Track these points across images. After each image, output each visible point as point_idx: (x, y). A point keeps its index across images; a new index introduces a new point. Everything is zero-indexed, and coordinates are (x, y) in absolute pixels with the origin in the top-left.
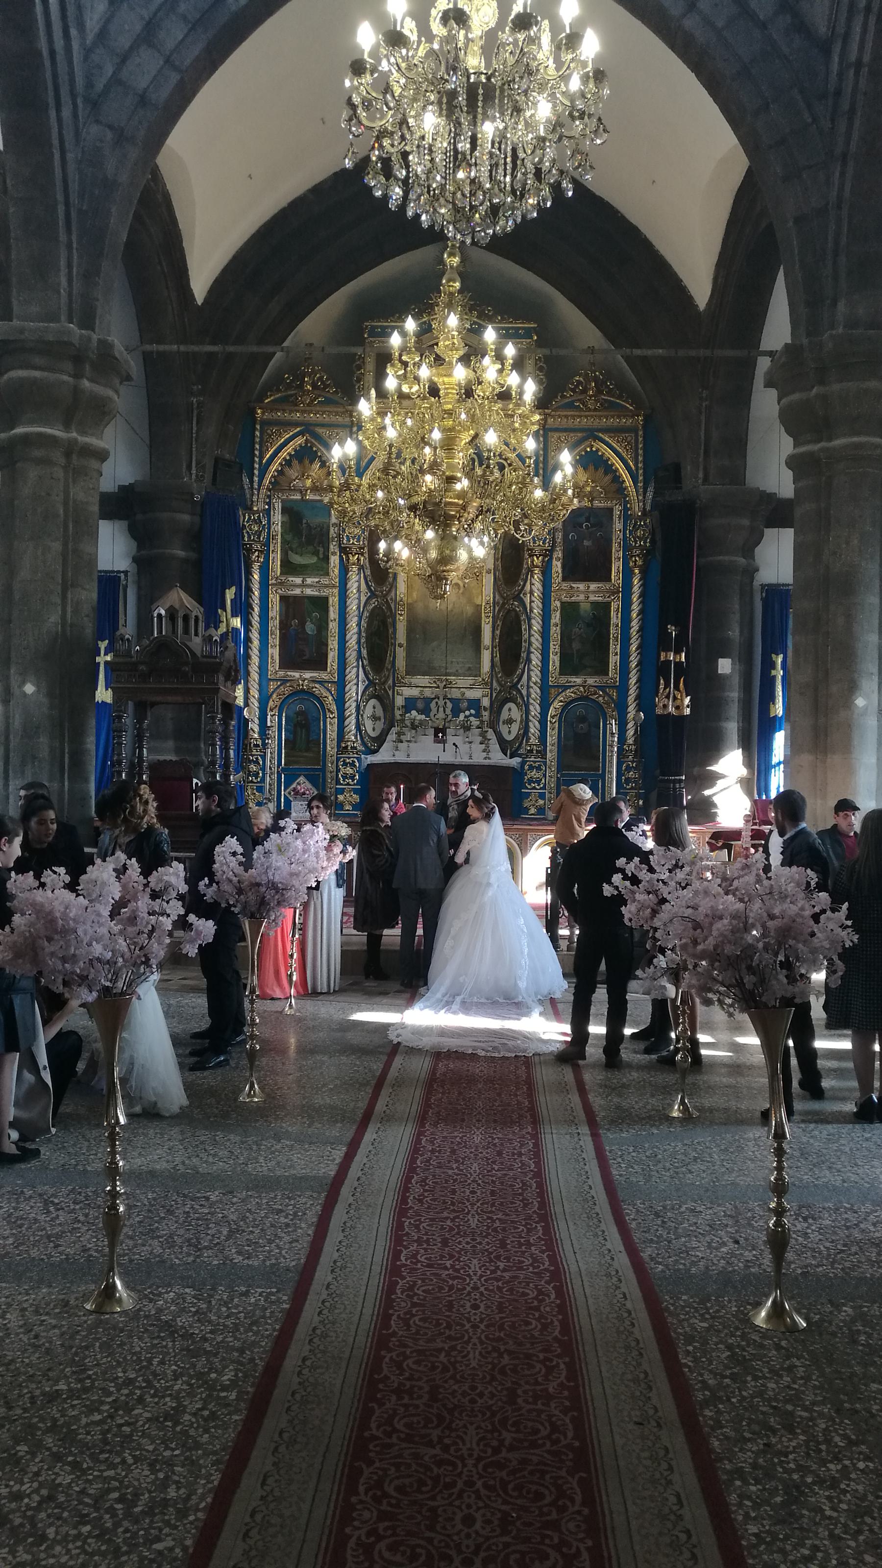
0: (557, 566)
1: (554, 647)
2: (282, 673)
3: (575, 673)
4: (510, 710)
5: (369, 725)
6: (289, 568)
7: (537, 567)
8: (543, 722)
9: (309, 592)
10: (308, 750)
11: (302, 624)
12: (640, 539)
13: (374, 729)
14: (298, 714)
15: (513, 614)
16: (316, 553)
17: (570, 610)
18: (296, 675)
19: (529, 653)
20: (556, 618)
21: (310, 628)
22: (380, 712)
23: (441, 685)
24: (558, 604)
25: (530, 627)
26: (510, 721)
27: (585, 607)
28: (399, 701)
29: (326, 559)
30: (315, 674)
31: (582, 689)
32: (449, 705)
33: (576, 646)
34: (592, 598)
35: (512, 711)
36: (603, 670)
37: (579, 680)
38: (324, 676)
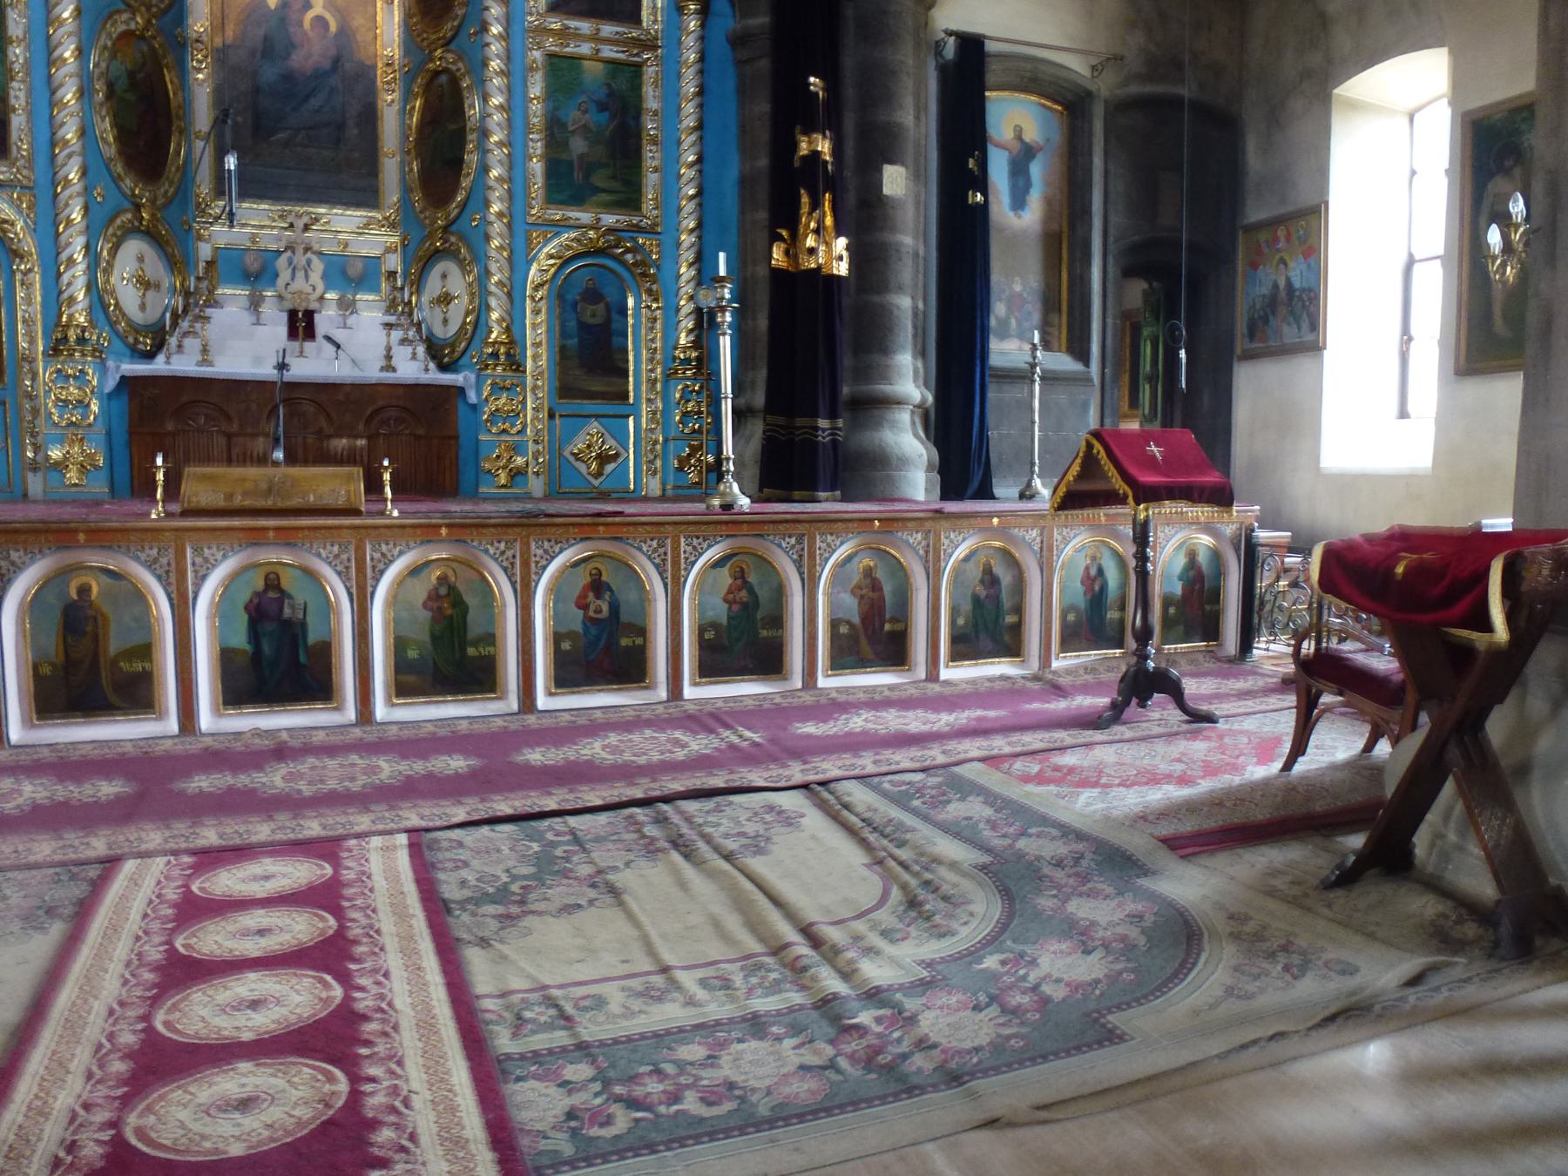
1: (537, 147)
3: (577, 200)
4: (444, 276)
5: (128, 297)
8: (513, 294)
13: (143, 307)
17: (561, 69)
19: (485, 152)
20: (536, 89)
22: (155, 267)
23: (300, 224)
24: (537, 54)
26: (445, 299)
27: (593, 69)
28: (205, 251)
32: (318, 266)
33: (578, 145)
34: (608, 52)
35: (449, 278)
36: (630, 199)
37: (585, 217)
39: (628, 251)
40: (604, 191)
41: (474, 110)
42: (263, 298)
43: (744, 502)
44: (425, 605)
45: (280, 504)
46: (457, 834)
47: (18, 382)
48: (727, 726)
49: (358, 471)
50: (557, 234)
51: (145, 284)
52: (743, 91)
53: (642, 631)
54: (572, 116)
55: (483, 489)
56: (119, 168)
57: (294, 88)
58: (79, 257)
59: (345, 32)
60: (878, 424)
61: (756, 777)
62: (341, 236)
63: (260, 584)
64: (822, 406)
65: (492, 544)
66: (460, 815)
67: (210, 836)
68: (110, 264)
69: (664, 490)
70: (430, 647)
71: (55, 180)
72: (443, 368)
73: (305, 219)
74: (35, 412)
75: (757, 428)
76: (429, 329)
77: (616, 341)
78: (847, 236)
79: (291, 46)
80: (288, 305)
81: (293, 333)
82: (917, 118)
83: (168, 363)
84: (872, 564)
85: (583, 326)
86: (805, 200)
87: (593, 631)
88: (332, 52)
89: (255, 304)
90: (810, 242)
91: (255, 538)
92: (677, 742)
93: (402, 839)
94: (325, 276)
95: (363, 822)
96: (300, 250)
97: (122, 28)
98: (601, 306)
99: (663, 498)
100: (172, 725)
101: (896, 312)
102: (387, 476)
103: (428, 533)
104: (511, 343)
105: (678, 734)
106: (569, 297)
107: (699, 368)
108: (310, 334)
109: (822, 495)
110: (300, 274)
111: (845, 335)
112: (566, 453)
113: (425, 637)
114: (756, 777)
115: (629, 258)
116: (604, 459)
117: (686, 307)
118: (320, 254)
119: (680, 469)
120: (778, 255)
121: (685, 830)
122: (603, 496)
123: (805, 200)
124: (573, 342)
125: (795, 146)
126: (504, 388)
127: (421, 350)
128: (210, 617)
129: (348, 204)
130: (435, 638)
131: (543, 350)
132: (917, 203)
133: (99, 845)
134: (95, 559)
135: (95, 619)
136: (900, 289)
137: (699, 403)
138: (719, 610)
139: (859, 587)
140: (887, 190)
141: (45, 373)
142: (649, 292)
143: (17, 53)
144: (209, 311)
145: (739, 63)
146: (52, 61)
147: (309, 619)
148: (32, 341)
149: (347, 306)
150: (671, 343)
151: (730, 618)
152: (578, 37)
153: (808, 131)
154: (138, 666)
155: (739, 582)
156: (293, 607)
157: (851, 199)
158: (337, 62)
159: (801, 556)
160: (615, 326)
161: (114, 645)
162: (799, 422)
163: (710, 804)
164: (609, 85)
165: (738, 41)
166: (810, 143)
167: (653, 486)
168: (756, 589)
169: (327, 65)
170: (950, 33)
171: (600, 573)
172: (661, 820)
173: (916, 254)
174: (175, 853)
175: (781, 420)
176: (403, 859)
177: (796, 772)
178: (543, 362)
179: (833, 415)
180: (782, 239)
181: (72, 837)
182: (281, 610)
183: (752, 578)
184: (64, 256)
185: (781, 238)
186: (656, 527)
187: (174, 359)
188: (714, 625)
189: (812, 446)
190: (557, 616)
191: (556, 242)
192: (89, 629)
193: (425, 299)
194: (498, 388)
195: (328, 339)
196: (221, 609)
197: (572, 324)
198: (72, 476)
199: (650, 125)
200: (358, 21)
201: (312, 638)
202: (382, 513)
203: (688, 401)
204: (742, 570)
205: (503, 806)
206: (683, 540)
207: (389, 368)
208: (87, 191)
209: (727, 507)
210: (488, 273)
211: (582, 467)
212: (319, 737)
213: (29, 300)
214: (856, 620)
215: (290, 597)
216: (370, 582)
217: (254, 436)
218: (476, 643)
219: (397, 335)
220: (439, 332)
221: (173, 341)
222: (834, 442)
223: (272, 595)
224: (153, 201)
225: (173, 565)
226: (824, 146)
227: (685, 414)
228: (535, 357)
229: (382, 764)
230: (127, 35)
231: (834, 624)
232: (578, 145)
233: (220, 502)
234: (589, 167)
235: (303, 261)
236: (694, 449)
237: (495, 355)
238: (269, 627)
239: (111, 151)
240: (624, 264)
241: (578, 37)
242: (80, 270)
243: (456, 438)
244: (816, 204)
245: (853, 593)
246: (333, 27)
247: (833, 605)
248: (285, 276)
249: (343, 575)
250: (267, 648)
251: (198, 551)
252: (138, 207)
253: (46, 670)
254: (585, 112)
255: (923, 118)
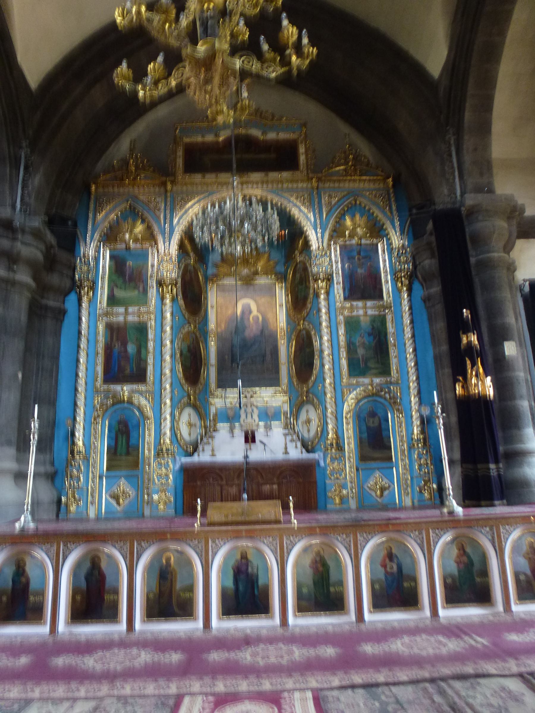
0: (338, 290)
1: (344, 354)
2: (106, 387)
3: (363, 373)
4: (307, 411)
5: (184, 430)
6: (112, 300)
7: (322, 288)
8: (338, 417)
9: (130, 318)
10: (128, 453)
11: (125, 344)
12: (406, 262)
13: (190, 434)
14: (120, 422)
15: (304, 332)
16: (136, 287)
18: (118, 388)
21: (131, 349)
22: (195, 419)
24: (341, 318)
25: (321, 338)
26: (308, 421)
28: (213, 410)
29: (145, 292)
30: (135, 387)
31: (370, 387)
32: (256, 412)
33: (361, 352)
34: (370, 312)
36: (385, 371)
37: (366, 380)
38: (142, 387)
39: (385, 393)
40: (373, 368)
41: (316, 344)
42: (235, 426)
43: (459, 510)
44: (310, 567)
45: (247, 519)
46: (335, 693)
47: (144, 468)
48: (466, 634)
49: (278, 503)
50: (355, 389)
51: (190, 425)
52: (431, 319)
53: (414, 579)
54: (357, 340)
55: (329, 506)
56: (183, 381)
57: (246, 345)
58: (168, 417)
59: (265, 320)
60: (521, 464)
61: (490, 668)
62: (265, 399)
63: (239, 557)
64: (491, 457)
65: (340, 535)
66: (336, 682)
67: (220, 687)
68: (179, 418)
69: (413, 502)
70: (312, 586)
71: (161, 388)
72: (308, 451)
73: (251, 393)
74: (149, 480)
75: (458, 470)
76: (302, 435)
77: (384, 433)
78: (490, 376)
79: (244, 328)
80: (244, 428)
81: (247, 441)
82: (516, 319)
83: (199, 455)
84: (532, 540)
85: (368, 428)
86: (468, 362)
87: (390, 578)
88: (260, 328)
89: (232, 430)
90: (474, 380)
91: (237, 536)
92: (440, 642)
93: (309, 695)
94: (259, 416)
95: (289, 683)
96: (249, 406)
97: (186, 330)
98: (376, 420)
99: (414, 508)
100: (200, 624)
101: (521, 409)
102: (291, 505)
103: (310, 532)
104: (338, 438)
105: (441, 638)
106: (362, 416)
107: (425, 443)
108: (254, 440)
109: (497, 502)
110: (249, 416)
111: (497, 422)
112: (366, 487)
113: (310, 582)
114: (490, 668)
115: (387, 396)
116: (383, 489)
117: (415, 415)
118: (257, 407)
119: (421, 492)
120: (459, 390)
121: (457, 699)
122: (385, 508)
123: (468, 362)
124: (365, 435)
125: (460, 340)
126: (336, 458)
127: (299, 444)
128: (218, 572)
129: (266, 386)
130: (315, 583)
131: (352, 441)
132: (523, 357)
133: (173, 689)
134: (173, 546)
135: (172, 573)
136: (521, 397)
137: (426, 460)
138: (453, 568)
139: (528, 554)
140: (507, 353)
141: (153, 464)
142: (398, 410)
143: (151, 345)
144: (214, 434)
145: (427, 308)
146: (162, 345)
147: (259, 574)
148: (149, 450)
149: (268, 428)
150: (410, 432)
151: (459, 571)
152: (357, 308)
153: (466, 332)
154: (187, 595)
155: (462, 552)
156: (252, 568)
157: (490, 359)
158: (262, 331)
159: (493, 537)
160: (383, 426)
161: (179, 585)
162: (479, 466)
163: (467, 684)
164: (373, 326)
165: (426, 300)
166: (467, 337)
167: (408, 502)
168: (472, 556)
169: (259, 333)
170: (525, 281)
171: (391, 548)
172: (442, 693)
173: (527, 380)
174: (206, 694)
175: (470, 466)
176: (311, 704)
177: (513, 666)
178: (352, 446)
179: (497, 462)
180: (459, 381)
181: (162, 682)
182: (247, 569)
183: (468, 550)
184: (163, 416)
185: (459, 381)
186: (417, 526)
187: (201, 454)
188: (452, 576)
189: (488, 478)
190: (372, 571)
191: (355, 392)
192: (169, 576)
193: (300, 422)
194: (333, 460)
195: (261, 442)
196: (223, 571)
197: (364, 428)
198: (161, 506)
199: (391, 340)
200: (270, 316)
201: (261, 582)
202: (290, 522)
203: (420, 459)
204: (462, 545)
205: (357, 678)
206: (431, 531)
207: (286, 452)
208: (172, 391)
209: (451, 513)
210: (326, 408)
211: (373, 494)
212: (264, 632)
213: (150, 435)
214: (529, 572)
215: (251, 562)
216: (286, 554)
217: (232, 486)
218: (334, 586)
219: (289, 438)
220: (306, 435)
221: (200, 447)
222: (499, 476)
223: (243, 561)
224: (195, 392)
225: (204, 547)
226: (474, 339)
227: (420, 465)
228: (348, 444)
229: (295, 649)
230: (188, 332)
231: (517, 575)
232: (361, 352)
233: (223, 519)
234: (366, 361)
235: (251, 410)
236: (426, 483)
237: (332, 444)
238: (242, 577)
239: (181, 375)
240: (385, 399)
241: (357, 308)
242: (168, 423)
243: (315, 482)
244: (474, 364)
245: (524, 556)
246: (260, 318)
247: (514, 564)
248: (243, 416)
249: (274, 552)
250: (241, 588)
251: (214, 542)
252: (189, 396)
253: (151, 596)
254: (363, 337)
255: (519, 318)
